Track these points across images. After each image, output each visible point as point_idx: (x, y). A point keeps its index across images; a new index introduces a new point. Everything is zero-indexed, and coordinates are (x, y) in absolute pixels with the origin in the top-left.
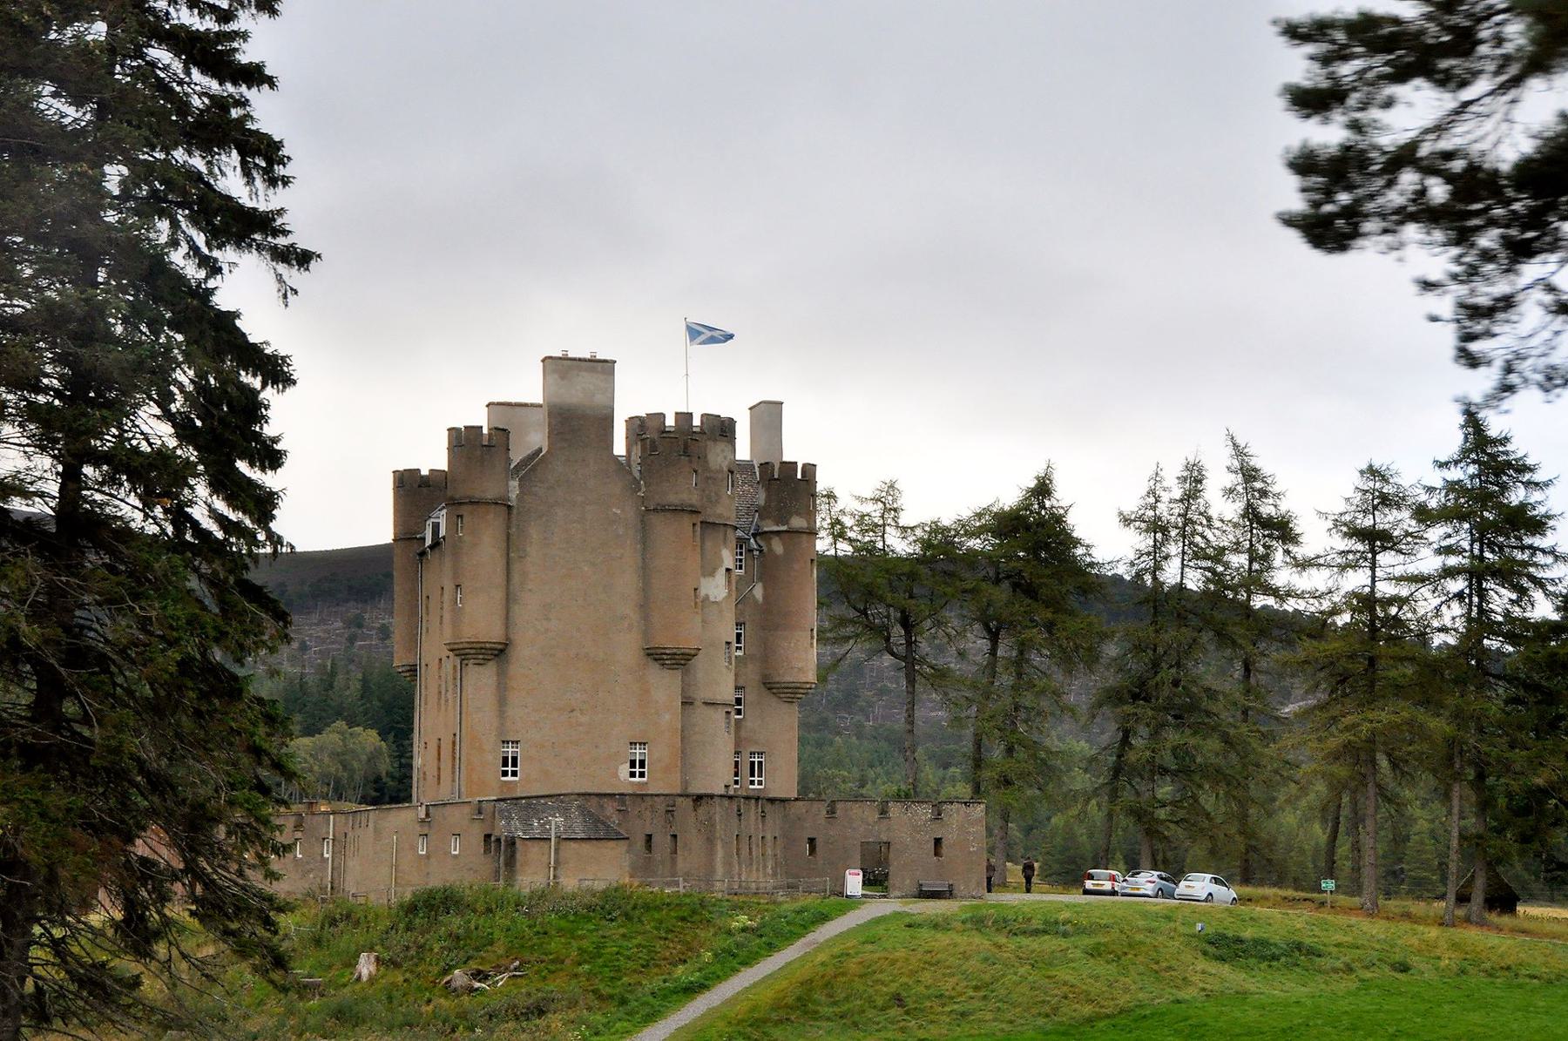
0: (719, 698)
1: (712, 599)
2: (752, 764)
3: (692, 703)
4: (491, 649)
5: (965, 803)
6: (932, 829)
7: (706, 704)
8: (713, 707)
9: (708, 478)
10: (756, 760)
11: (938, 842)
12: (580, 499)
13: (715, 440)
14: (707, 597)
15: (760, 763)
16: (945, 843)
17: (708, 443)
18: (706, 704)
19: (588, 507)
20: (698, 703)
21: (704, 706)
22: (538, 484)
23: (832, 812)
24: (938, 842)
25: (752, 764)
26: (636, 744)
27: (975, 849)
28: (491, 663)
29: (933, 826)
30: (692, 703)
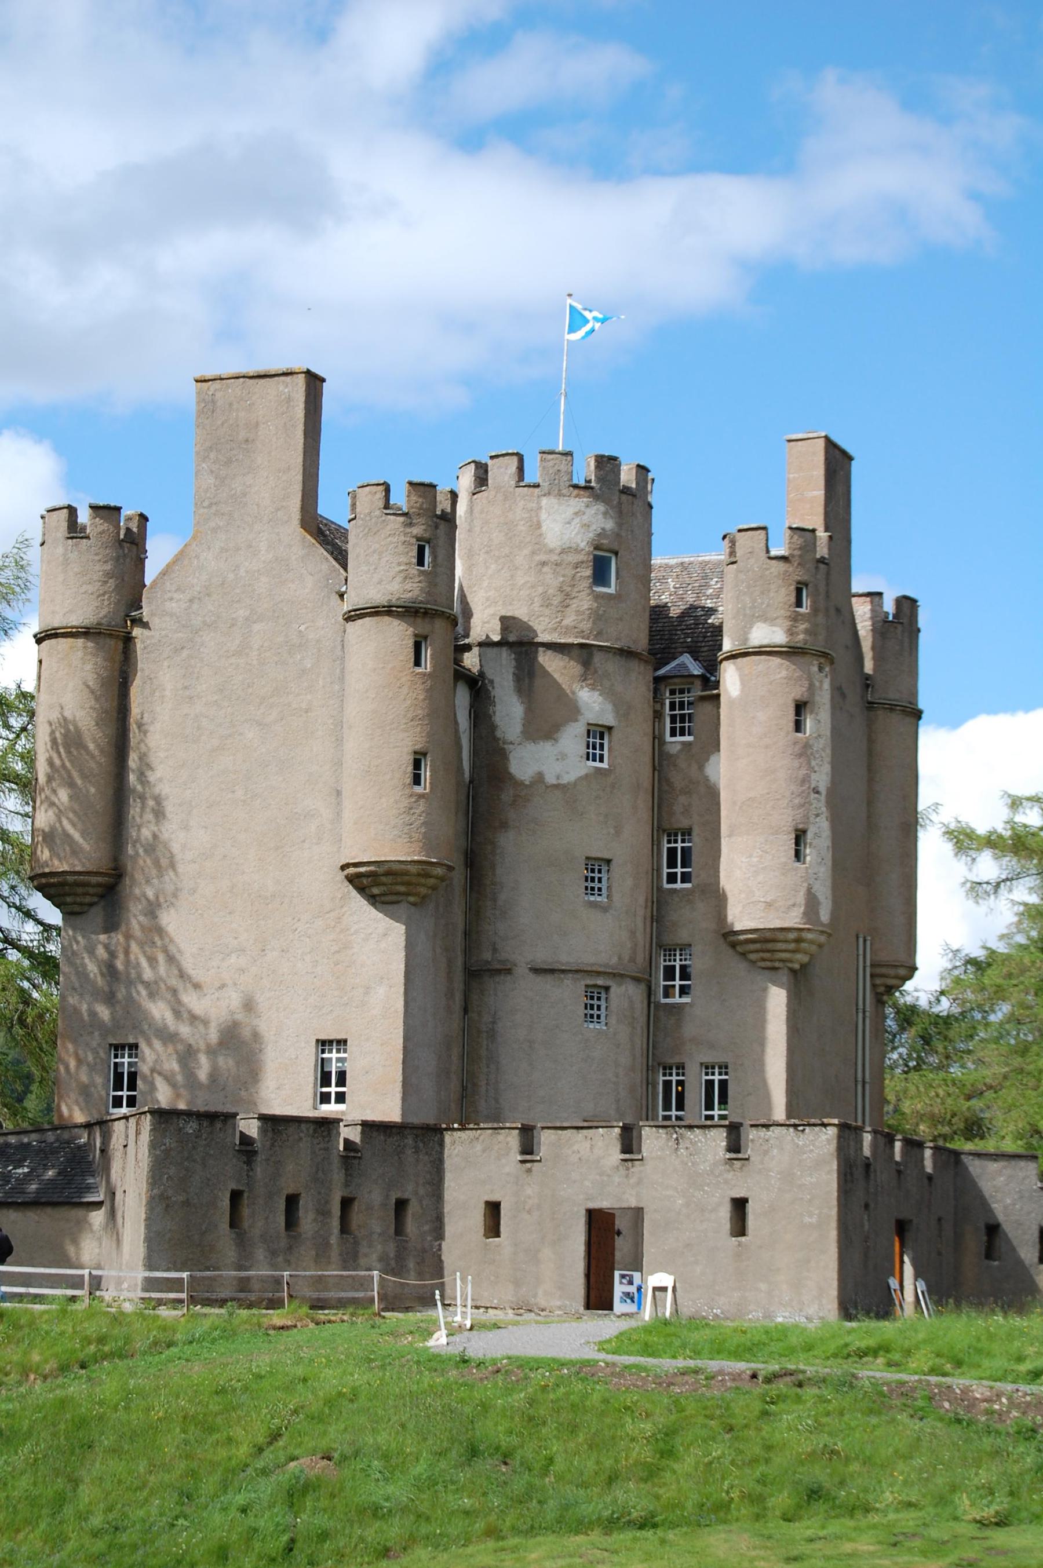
0: (565, 958)
1: (550, 779)
2: (710, 1084)
3: (509, 971)
4: (77, 884)
5: (795, 1126)
6: (726, 1182)
7: (537, 971)
8: (549, 978)
9: (544, 564)
10: (716, 1078)
11: (740, 1205)
12: (242, 613)
13: (560, 495)
14: (540, 777)
15: (723, 1084)
16: (750, 1207)
17: (544, 501)
18: (537, 971)
19: (256, 627)
20: (522, 970)
21: (532, 976)
22: (176, 596)
23: (528, 1148)
24: (740, 1205)
25: (710, 1084)
26: (331, 1042)
27: (814, 1220)
28: (94, 910)
29: (730, 1175)
30: (509, 971)
